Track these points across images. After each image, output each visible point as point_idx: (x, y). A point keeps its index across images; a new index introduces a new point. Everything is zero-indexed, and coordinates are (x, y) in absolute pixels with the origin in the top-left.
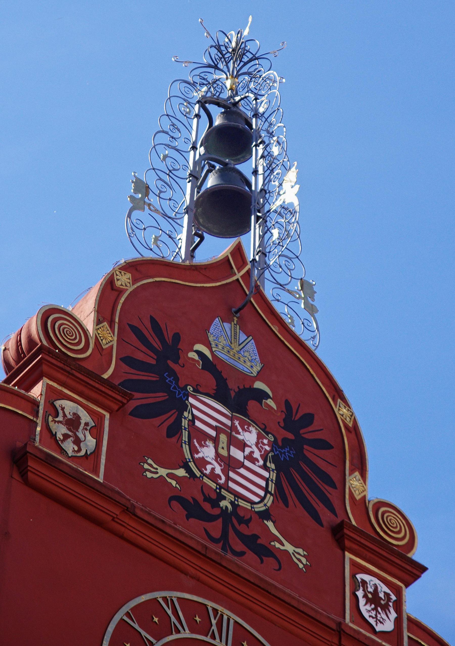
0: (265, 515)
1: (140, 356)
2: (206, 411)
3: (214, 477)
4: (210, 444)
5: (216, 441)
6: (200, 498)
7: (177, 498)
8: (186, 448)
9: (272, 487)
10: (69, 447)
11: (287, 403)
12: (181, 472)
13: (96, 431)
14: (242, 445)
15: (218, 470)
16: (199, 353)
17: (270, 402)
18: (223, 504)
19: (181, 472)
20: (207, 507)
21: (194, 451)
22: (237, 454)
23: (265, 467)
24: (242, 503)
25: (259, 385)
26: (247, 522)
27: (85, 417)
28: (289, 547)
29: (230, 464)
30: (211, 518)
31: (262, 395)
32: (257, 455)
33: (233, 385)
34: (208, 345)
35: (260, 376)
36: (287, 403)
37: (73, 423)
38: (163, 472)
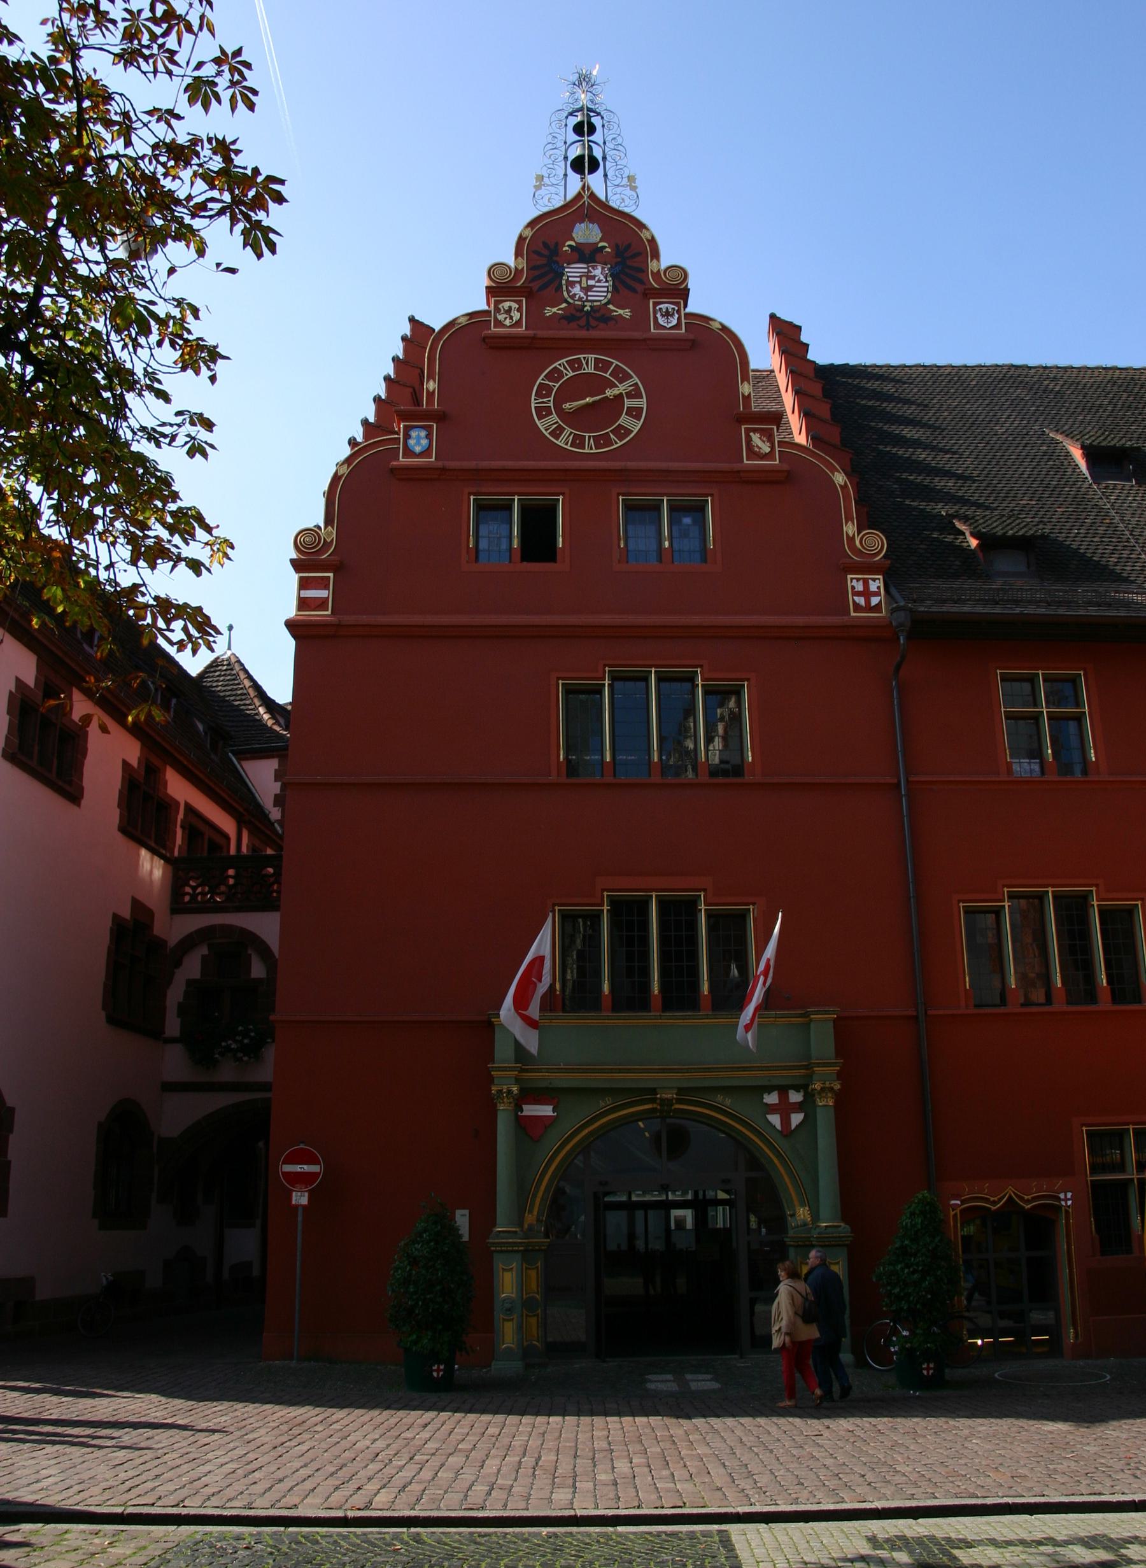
0: (608, 303)
1: (539, 263)
2: (574, 271)
3: (580, 299)
4: (578, 286)
5: (580, 282)
6: (574, 312)
7: (562, 317)
8: (565, 294)
9: (610, 289)
10: (508, 322)
11: (617, 246)
12: (564, 305)
13: (519, 310)
14: (593, 278)
15: (582, 295)
16: (569, 246)
17: (608, 250)
19: (564, 305)
20: (578, 314)
21: (568, 292)
22: (591, 282)
23: (607, 281)
25: (600, 245)
26: (598, 311)
27: (515, 306)
28: (621, 312)
29: (589, 289)
30: (579, 318)
31: (605, 247)
32: (602, 277)
33: (587, 252)
34: (573, 239)
35: (601, 240)
36: (617, 246)
38: (554, 310)
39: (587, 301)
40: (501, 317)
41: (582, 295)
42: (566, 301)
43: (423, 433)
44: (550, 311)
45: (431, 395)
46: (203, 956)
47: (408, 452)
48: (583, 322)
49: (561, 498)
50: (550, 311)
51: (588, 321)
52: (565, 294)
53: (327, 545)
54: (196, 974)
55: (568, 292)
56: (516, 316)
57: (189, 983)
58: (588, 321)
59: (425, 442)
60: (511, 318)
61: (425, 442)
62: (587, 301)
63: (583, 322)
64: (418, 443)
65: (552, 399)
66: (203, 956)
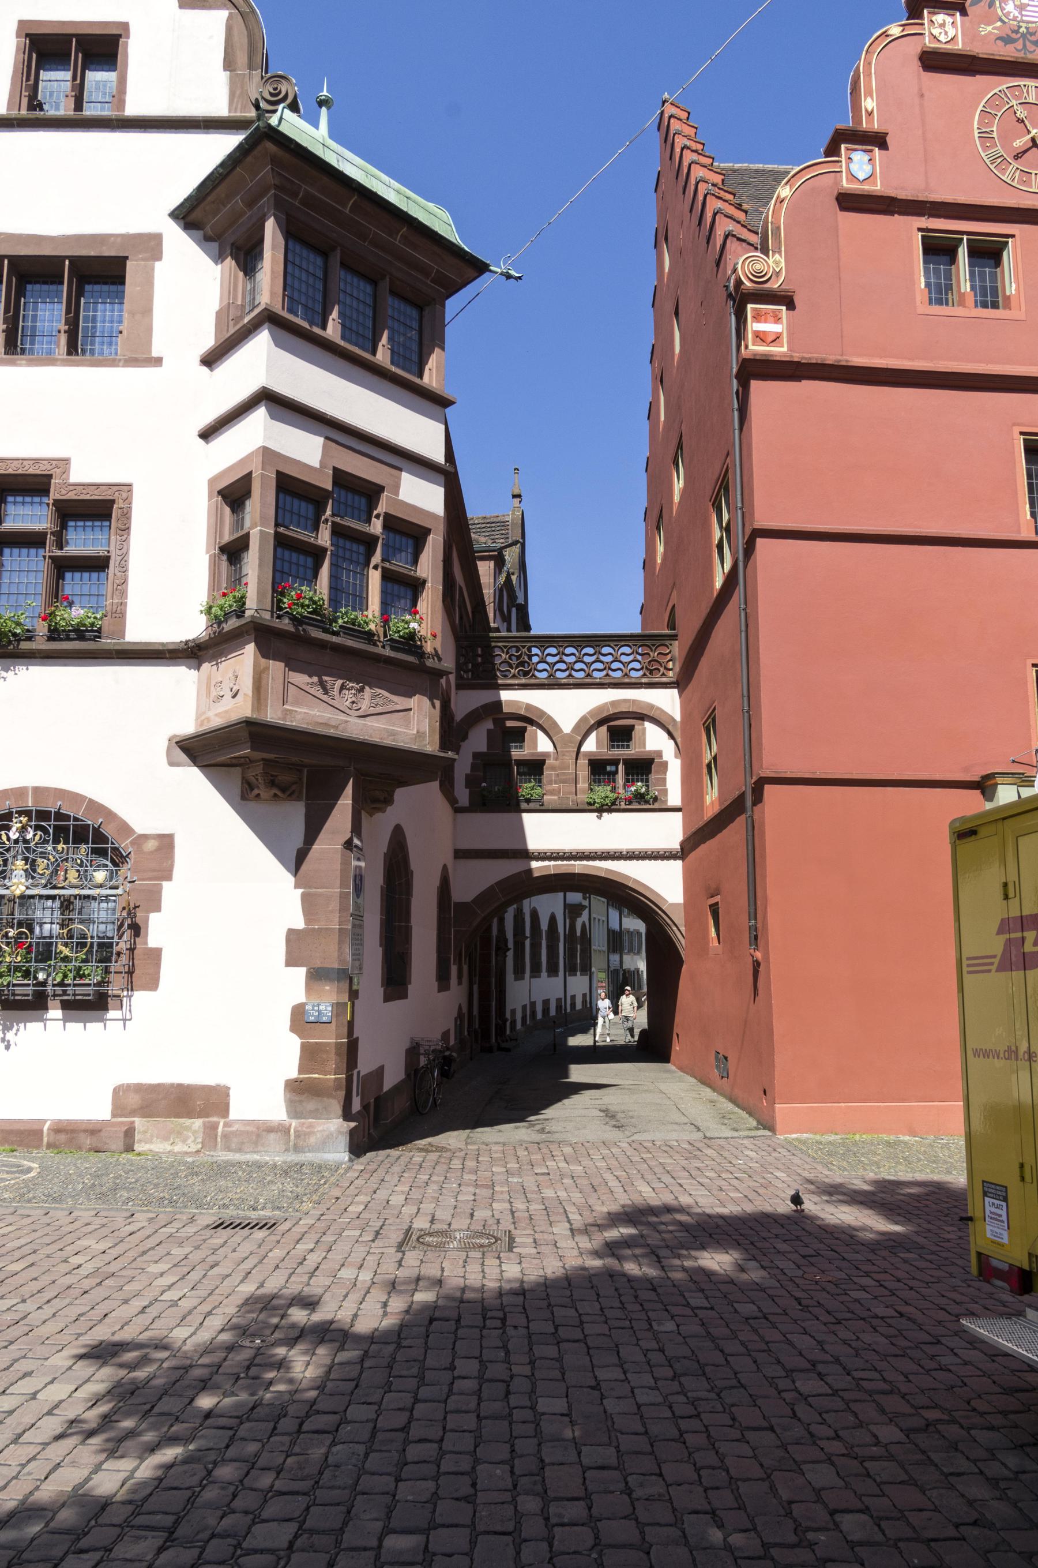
3: (1015, 19)
6: (1009, 33)
8: (999, 10)
10: (943, 38)
15: (1017, 14)
18: (1021, 30)
20: (1014, 36)
21: (1002, 9)
24: (1030, 25)
37: (942, 25)
38: (989, 28)
39: (1023, 22)
40: (936, 32)
41: (1017, 14)
42: (1001, 20)
43: (866, 158)
44: (986, 29)
45: (870, 114)
46: (489, 731)
47: (852, 177)
48: (1019, 45)
49: (1010, 240)
50: (986, 29)
51: (1024, 46)
52: (999, 10)
53: (778, 274)
54: (483, 748)
55: (1002, 9)
56: (951, 33)
57: (476, 755)
58: (1024, 46)
59: (868, 169)
60: (946, 33)
61: (868, 169)
62: (1023, 22)
63: (1019, 45)
64: (861, 168)
65: (995, 129)
66: (489, 731)
